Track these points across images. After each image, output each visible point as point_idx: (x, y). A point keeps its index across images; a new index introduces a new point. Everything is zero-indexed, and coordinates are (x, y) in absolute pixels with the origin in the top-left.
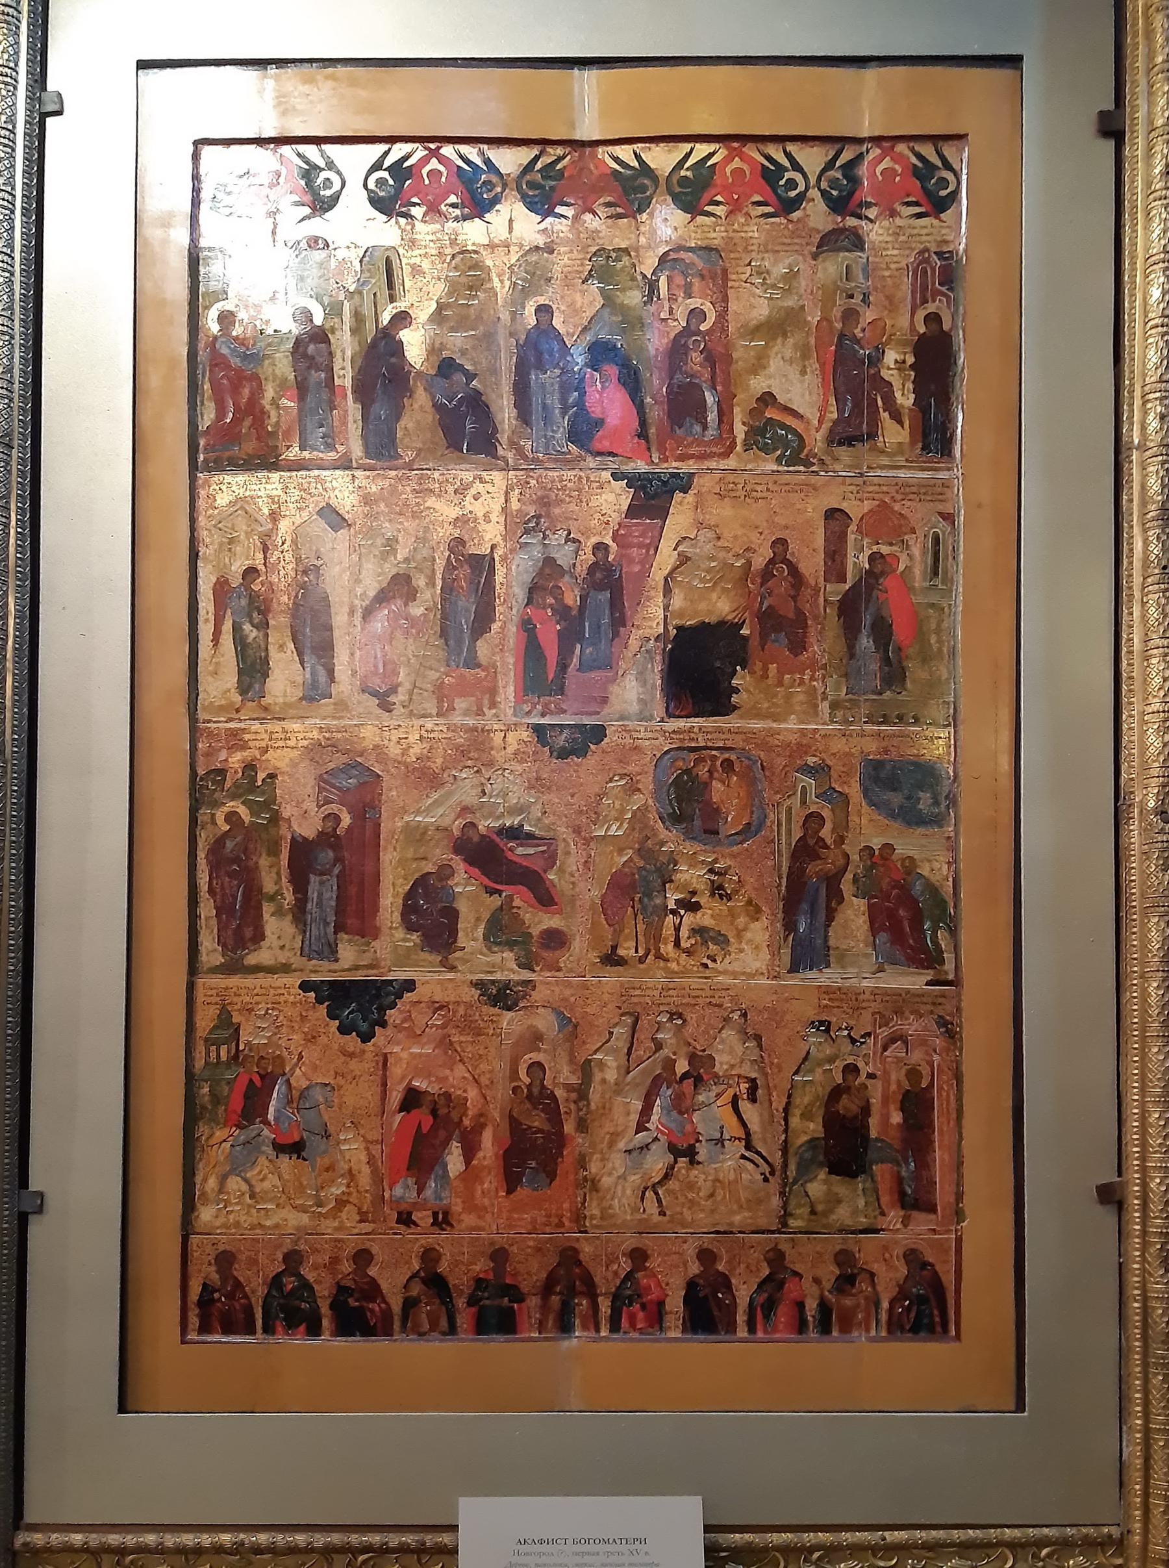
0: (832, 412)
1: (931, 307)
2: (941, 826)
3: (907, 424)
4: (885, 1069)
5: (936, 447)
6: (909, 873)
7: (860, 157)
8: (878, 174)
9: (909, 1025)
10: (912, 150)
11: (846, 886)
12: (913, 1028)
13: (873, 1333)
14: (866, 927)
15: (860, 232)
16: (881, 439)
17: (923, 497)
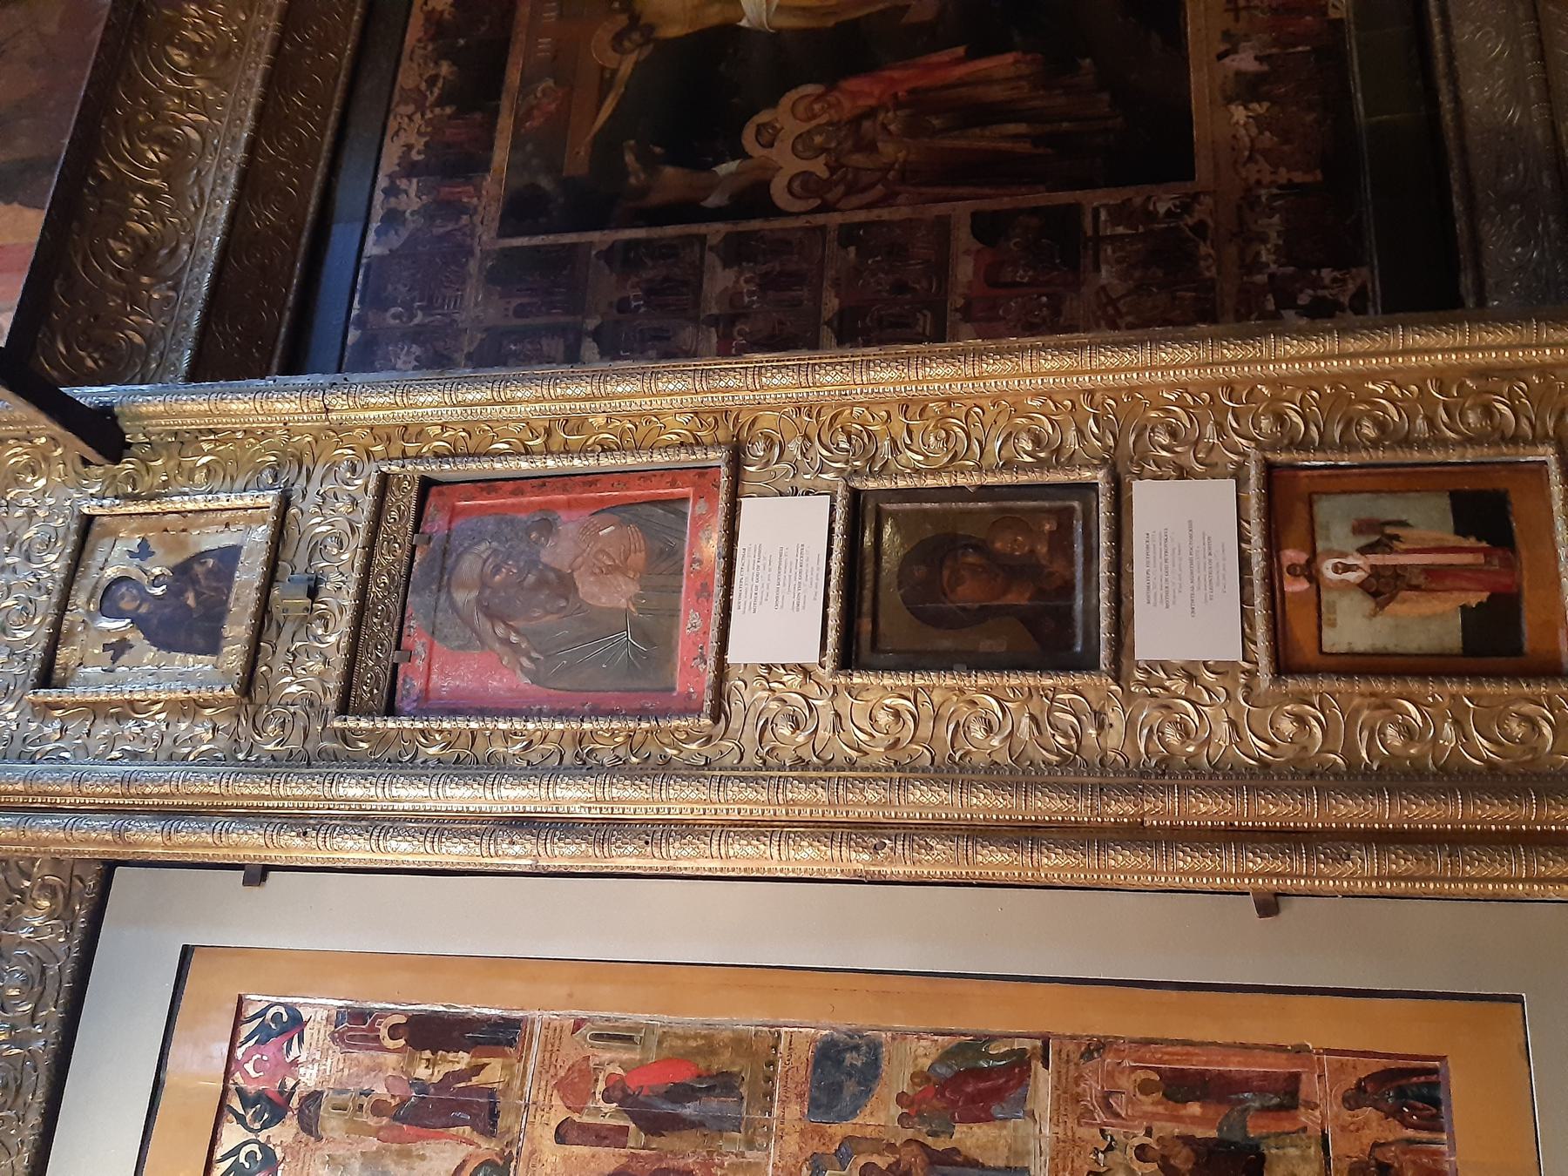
0: (464, 1132)
1: (384, 1032)
2: (881, 1045)
3: (485, 1060)
4: (1140, 1117)
5: (511, 1033)
6: (928, 1079)
7: (240, 1091)
8: (257, 1075)
9: (1091, 1088)
10: (243, 1044)
11: (940, 1144)
12: (1094, 1084)
13: (1445, 1148)
14: (985, 1127)
15: (305, 1094)
16: (495, 1085)
17: (556, 1048)
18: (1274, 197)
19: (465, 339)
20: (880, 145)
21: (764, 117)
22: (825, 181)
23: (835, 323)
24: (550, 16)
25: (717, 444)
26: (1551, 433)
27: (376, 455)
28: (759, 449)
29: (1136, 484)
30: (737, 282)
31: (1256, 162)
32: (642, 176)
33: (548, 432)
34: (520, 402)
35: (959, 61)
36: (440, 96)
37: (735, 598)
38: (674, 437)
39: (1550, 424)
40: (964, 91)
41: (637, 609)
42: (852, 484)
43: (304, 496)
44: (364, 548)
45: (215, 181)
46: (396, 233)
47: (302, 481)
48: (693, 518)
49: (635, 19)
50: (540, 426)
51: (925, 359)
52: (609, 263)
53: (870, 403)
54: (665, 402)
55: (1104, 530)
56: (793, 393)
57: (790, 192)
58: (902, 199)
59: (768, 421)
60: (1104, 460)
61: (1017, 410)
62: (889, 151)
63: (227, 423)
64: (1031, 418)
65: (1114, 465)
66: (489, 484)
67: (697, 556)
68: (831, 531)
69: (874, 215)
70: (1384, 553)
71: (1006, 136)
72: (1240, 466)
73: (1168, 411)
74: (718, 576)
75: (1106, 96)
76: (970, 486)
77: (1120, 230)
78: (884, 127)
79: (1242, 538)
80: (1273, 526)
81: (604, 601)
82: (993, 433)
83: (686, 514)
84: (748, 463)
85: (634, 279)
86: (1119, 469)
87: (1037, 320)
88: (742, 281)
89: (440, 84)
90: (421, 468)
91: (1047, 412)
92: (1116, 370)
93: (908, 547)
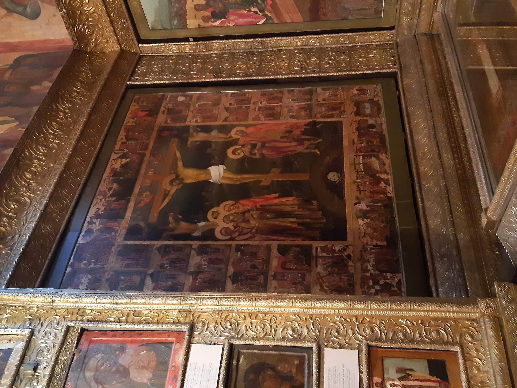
18: (371, 249)
19: (107, 274)
20: (251, 221)
21: (215, 209)
22: (232, 231)
23: (232, 277)
24: (151, 173)
25: (185, 323)
26: (458, 342)
27: (67, 318)
28: (200, 326)
29: (326, 349)
30: (201, 261)
31: (366, 237)
32: (174, 224)
33: (128, 315)
34: (120, 304)
35: (276, 198)
36: (112, 194)
37: (185, 382)
38: (171, 320)
39: (458, 338)
40: (278, 207)
41: (150, 383)
42: (230, 342)
43: (39, 332)
44: (56, 353)
45: (32, 215)
46: (90, 237)
47: (39, 326)
48: (174, 350)
49: (177, 177)
50: (126, 312)
51: (258, 299)
52: (159, 252)
53: (239, 312)
54: (170, 307)
55: (315, 365)
56: (213, 307)
57: (221, 233)
58: (256, 238)
59: (204, 316)
60: (315, 339)
61: (288, 319)
62: (253, 223)
63: (17, 303)
64: (292, 322)
65: (319, 342)
66: (104, 332)
67: (174, 364)
68: (222, 358)
69: (247, 242)
70: (406, 380)
71: (289, 222)
72: (360, 345)
73: (336, 324)
74: (180, 373)
75: (320, 213)
76: (271, 345)
77: (324, 254)
78: (252, 215)
79: (360, 371)
80: (370, 368)
81: (139, 380)
82: (279, 326)
83: (172, 348)
84: (196, 331)
85: (167, 258)
86: (321, 343)
87: (297, 282)
88: (202, 261)
89: (112, 190)
90: (82, 325)
91: (297, 320)
92: (319, 308)
93: (248, 366)
